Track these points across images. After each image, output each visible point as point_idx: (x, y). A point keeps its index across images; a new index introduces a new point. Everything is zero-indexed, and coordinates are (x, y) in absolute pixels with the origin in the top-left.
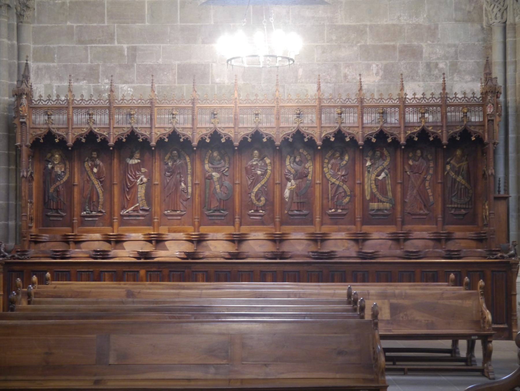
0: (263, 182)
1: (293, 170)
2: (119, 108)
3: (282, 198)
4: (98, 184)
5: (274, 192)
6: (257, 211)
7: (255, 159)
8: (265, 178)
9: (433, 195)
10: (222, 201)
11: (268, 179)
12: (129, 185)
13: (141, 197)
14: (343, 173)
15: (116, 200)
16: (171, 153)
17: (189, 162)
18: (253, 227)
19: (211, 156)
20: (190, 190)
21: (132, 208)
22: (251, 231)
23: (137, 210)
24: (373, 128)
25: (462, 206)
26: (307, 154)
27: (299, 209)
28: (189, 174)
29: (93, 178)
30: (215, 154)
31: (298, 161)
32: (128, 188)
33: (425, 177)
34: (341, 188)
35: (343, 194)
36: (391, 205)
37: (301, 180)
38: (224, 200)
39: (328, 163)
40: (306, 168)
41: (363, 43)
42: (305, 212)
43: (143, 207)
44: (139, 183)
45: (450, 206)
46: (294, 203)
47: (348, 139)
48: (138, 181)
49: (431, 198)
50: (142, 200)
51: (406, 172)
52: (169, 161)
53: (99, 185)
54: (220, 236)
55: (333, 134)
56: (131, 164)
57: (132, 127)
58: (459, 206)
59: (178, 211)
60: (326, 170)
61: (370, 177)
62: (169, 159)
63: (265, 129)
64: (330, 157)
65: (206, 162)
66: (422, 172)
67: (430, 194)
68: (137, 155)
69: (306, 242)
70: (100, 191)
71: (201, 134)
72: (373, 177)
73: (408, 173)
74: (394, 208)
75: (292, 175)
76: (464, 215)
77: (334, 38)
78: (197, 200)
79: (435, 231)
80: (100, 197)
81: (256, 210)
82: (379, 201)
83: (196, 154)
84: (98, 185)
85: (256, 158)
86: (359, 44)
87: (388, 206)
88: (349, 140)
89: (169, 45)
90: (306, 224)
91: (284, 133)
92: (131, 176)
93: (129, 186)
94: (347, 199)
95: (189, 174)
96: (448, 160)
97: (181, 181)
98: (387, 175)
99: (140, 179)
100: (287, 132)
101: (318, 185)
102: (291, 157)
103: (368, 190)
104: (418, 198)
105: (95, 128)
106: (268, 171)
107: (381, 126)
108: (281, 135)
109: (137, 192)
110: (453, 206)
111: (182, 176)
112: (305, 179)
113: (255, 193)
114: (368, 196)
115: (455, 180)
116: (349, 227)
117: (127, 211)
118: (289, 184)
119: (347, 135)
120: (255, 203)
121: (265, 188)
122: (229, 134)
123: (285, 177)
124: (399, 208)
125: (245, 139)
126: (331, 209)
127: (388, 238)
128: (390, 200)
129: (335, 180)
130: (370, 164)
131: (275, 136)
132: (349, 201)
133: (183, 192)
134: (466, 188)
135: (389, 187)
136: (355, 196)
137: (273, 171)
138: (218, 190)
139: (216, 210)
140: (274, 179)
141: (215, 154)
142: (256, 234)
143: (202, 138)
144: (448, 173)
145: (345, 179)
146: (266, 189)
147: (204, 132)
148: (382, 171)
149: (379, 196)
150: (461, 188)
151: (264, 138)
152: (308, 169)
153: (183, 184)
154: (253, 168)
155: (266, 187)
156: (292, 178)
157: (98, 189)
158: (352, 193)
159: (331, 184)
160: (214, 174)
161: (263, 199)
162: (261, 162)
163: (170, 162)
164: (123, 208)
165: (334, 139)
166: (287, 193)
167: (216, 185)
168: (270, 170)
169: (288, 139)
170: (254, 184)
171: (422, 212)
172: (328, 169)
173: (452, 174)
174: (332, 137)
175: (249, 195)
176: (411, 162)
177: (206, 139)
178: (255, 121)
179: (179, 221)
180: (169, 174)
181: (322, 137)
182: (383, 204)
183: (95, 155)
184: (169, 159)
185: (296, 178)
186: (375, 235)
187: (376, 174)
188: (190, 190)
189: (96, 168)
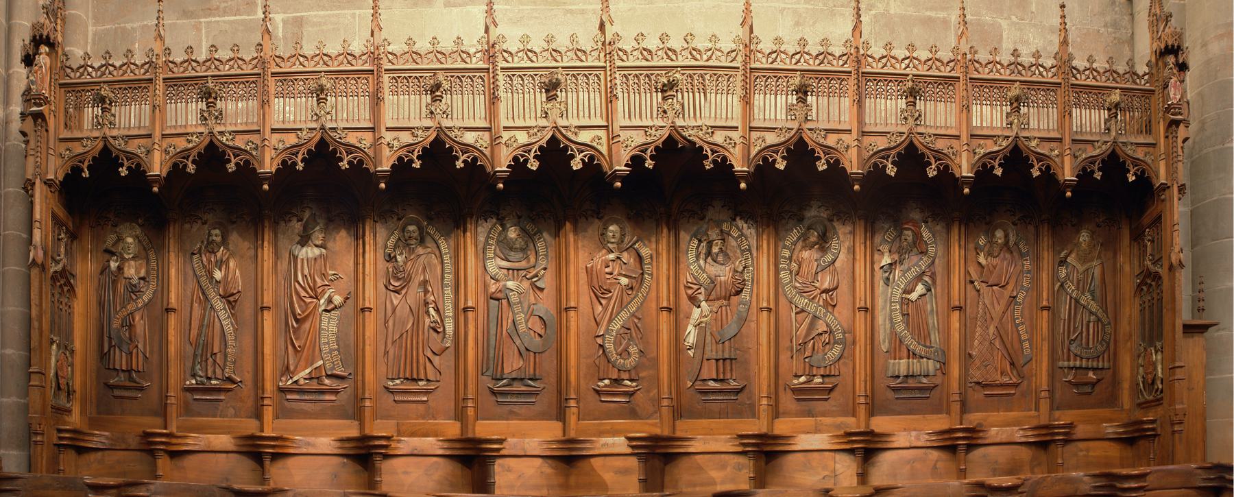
4: (224, 309)
5: (658, 331)
6: (617, 381)
8: (640, 295)
13: (328, 343)
15: (268, 349)
17: (446, 254)
20: (450, 327)
21: (308, 371)
27: (721, 377)
28: (447, 286)
29: (212, 294)
31: (717, 255)
32: (297, 321)
37: (725, 302)
42: (733, 384)
43: (333, 368)
44: (323, 308)
46: (708, 360)
48: (322, 301)
50: (331, 351)
51: (972, 282)
53: (227, 312)
56: (302, 260)
59: (422, 380)
66: (1007, 283)
72: (898, 293)
75: (702, 289)
80: (230, 343)
82: (911, 354)
93: (299, 314)
94: (836, 351)
95: (447, 286)
99: (326, 296)
102: (700, 241)
104: (997, 343)
110: (1072, 364)
113: (614, 334)
114: (884, 342)
115: (1077, 301)
117: (295, 379)
120: (615, 361)
121: (636, 321)
124: (955, 370)
134: (1099, 320)
135: (932, 321)
139: (514, 379)
141: (512, 233)
144: (1062, 285)
145: (832, 299)
149: (909, 340)
150: (1089, 322)
153: (432, 311)
155: (639, 319)
156: (701, 297)
159: (797, 313)
160: (510, 284)
163: (401, 254)
164: (286, 371)
166: (691, 335)
167: (518, 313)
168: (649, 274)
171: (1005, 380)
176: (982, 260)
179: (421, 407)
184: (395, 247)
188: (450, 327)
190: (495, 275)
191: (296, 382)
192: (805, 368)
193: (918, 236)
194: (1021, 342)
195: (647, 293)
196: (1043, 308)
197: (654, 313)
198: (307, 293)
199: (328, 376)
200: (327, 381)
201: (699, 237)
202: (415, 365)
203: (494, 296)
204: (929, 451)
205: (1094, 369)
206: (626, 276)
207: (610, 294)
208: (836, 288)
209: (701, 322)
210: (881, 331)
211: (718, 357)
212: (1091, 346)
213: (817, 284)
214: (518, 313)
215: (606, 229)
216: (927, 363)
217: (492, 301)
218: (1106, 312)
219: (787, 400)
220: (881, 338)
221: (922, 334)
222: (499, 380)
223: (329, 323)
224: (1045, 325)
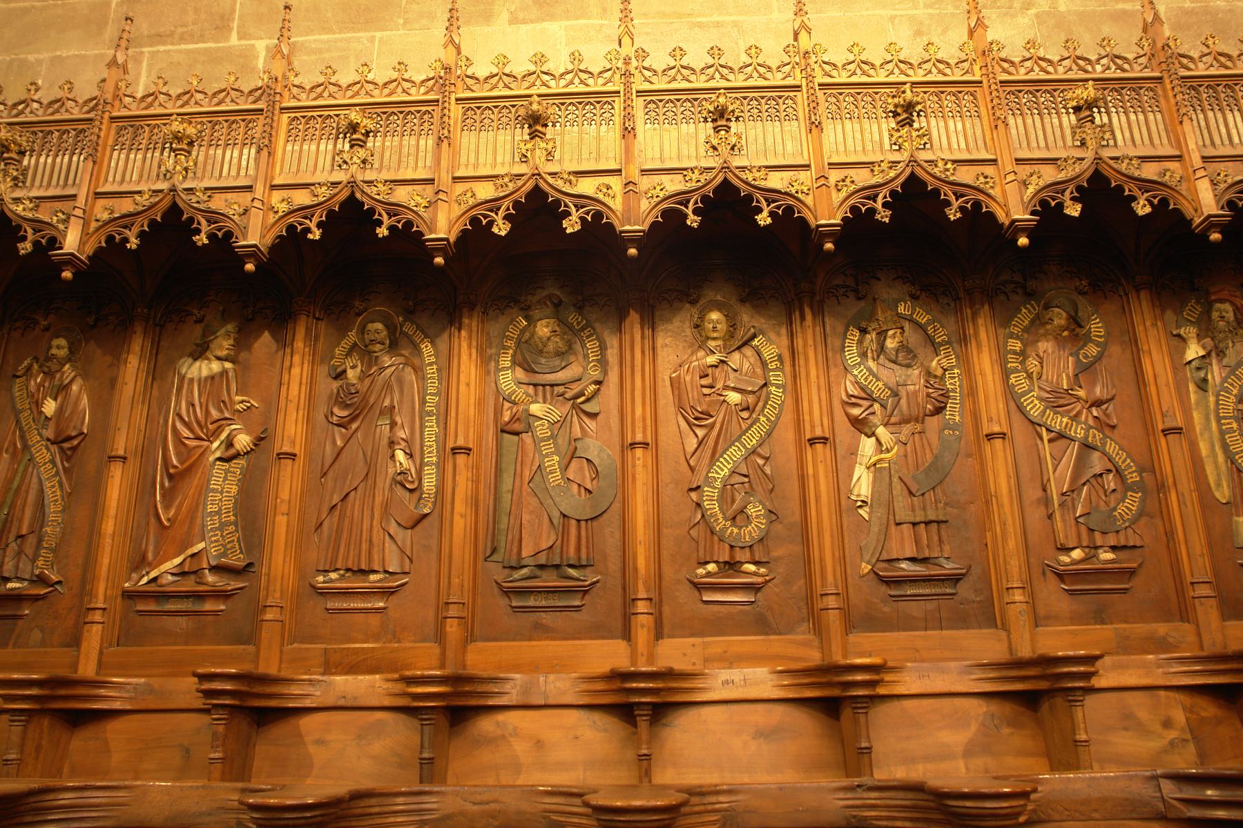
0: (751, 439)
1: (881, 384)
2: (133, 122)
3: (844, 504)
4: (53, 461)
6: (731, 566)
7: (712, 344)
8: (762, 418)
10: (573, 522)
11: (773, 426)
12: (175, 462)
13: (219, 513)
14: (1098, 392)
15: (109, 526)
16: (363, 330)
17: (431, 364)
18: (718, 644)
19: (527, 335)
21: (177, 561)
22: (707, 660)
23: (195, 572)
26: (929, 323)
28: (430, 414)
30: (543, 329)
32: (171, 477)
34: (1096, 455)
37: (919, 427)
38: (579, 521)
39: (1023, 354)
40: (936, 377)
42: (949, 567)
43: (224, 555)
44: (218, 454)
48: (216, 444)
50: (222, 526)
52: (349, 363)
53: (55, 465)
54: (559, 686)
55: (1071, 187)
56: (192, 380)
57: (173, 189)
60: (1018, 381)
61: (1212, 406)
62: (349, 354)
64: (1026, 330)
65: (506, 361)
68: (223, 345)
69: (978, 708)
70: (53, 494)
71: (471, 202)
75: (876, 406)
78: (460, 524)
81: (726, 563)
83: (460, 330)
84: (49, 466)
85: (714, 339)
86: (1032, 11)
89: (401, 32)
90: (961, 620)
91: (852, 188)
92: (187, 425)
93: (175, 467)
94: (1130, 504)
95: (430, 414)
97: (392, 443)
99: (223, 436)
100: (861, 185)
102: (864, 331)
105: (17, 200)
106: (773, 389)
108: (837, 197)
109: (204, 489)
111: (398, 419)
112: (933, 422)
113: (718, 484)
114: (1219, 485)
116: (1162, 629)
117: (153, 574)
118: (867, 445)
119: (1137, 192)
120: (725, 528)
121: (761, 462)
122: (600, 196)
123: (847, 415)
125: (671, 218)
129: (1065, 420)
131: (809, 200)
132: (1142, 513)
133: (399, 489)
136: (1161, 487)
138: (555, 478)
141: (543, 329)
142: (736, 674)
143: (474, 221)
145: (1107, 416)
146: (768, 470)
147: (485, 191)
151: (760, 210)
152: (942, 378)
153: (400, 455)
154: (704, 382)
155: (767, 459)
157: (47, 484)
158: (1144, 474)
159: (1050, 441)
160: (535, 409)
162: (736, 355)
163: (353, 367)
164: (140, 562)
165: (1079, 207)
166: (863, 484)
167: (547, 455)
168: (778, 386)
169: (872, 211)
172: (1030, 376)
175: (694, 495)
177: (491, 223)
178: (715, 142)
179: (374, 620)
180: (345, 413)
183: (58, 347)
185: (893, 420)
187: (1235, 392)
189: (55, 399)
190: (510, 395)
191: (155, 579)
192: (1079, 536)
195: (778, 417)
197: (792, 449)
198: (191, 430)
199: (215, 569)
200: (210, 578)
201: (863, 324)
202: (364, 546)
203: (506, 428)
206: (735, 389)
207: (711, 420)
208: (1112, 399)
210: (1209, 470)
211: (918, 520)
213: (1081, 393)
214: (547, 455)
215: (702, 318)
217: (506, 436)
219: (1053, 595)
220: (1212, 480)
222: (512, 568)
223: (225, 479)
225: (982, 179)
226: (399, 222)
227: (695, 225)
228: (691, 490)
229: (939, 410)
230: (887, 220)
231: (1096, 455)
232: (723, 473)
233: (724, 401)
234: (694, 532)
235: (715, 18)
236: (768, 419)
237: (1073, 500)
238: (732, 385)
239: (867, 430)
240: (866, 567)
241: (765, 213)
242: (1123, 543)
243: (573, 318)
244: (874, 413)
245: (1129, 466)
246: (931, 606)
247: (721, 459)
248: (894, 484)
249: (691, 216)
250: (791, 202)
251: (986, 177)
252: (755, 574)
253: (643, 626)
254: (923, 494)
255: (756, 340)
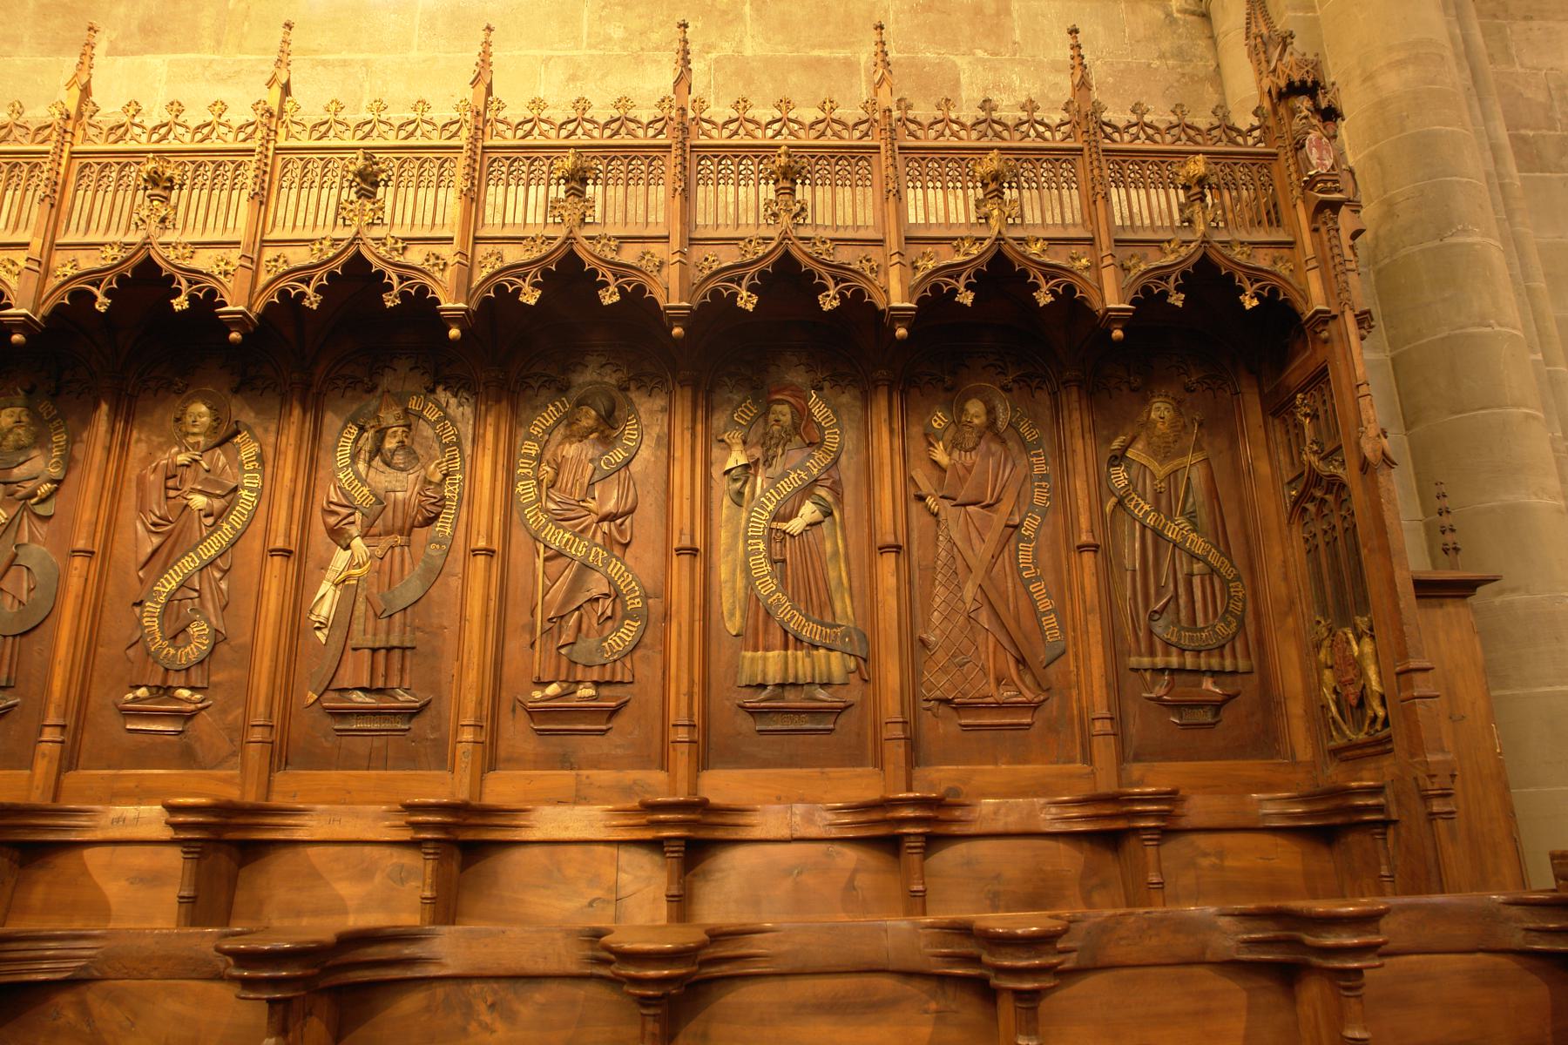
0: (210, 549)
1: (366, 490)
5: (259, 594)
8: (226, 526)
9: (1059, 612)
24: (742, 244)
25: (1203, 663)
27: (380, 684)
33: (1017, 520)
35: (606, 606)
36: (852, 665)
37: (400, 539)
41: (727, 48)
42: (404, 699)
45: (1146, 661)
46: (355, 649)
47: (609, 297)
49: (1050, 622)
51: (921, 498)
58: (1189, 661)
63: (187, 252)
66: (998, 500)
67: (1044, 604)
72: (761, 520)
73: (930, 500)
74: (865, 664)
75: (358, 515)
76: (1217, 706)
77: (617, 32)
79: (1084, 790)
81: (159, 688)
82: (791, 640)
85: (194, 434)
86: (713, 55)
87: (836, 664)
88: (616, 298)
94: (627, 633)
96: (1116, 444)
98: (828, 513)
100: (293, 265)
101: (481, 560)
102: (362, 429)
103: (734, 589)
104: (984, 618)
107: (785, 237)
110: (1159, 661)
113: (162, 599)
114: (732, 614)
115: (1158, 534)
118: (341, 558)
119: (610, 278)
121: (218, 575)
123: (325, 523)
124: (891, 673)
126: (542, 684)
127: (835, 833)
128: (847, 634)
130: (743, 461)
134: (1213, 571)
135: (837, 573)
137: (265, 495)
140: (267, 531)
142: (130, 811)
144: (1120, 503)
145: (621, 533)
146: (223, 585)
148: (806, 491)
149: (785, 611)
150: (1190, 575)
151: (178, 293)
155: (225, 572)
156: (354, 530)
159: (546, 560)
161: (199, 631)
166: (326, 601)
168: (251, 490)
170: (159, 561)
171: (1007, 694)
173: (1142, 507)
174: (527, 288)
175: (137, 610)
176: (940, 455)
181: (475, 284)
182: (808, 655)
186: (769, 822)
187: (771, 507)
192: (558, 668)
193: (802, 416)
194: (1036, 615)
196: (1081, 548)
204: (837, 847)
205: (1213, 673)
206: (201, 492)
208: (631, 511)
209: (349, 577)
211: (377, 645)
212: (1200, 624)
213: (592, 505)
216: (828, 659)
218: (1227, 553)
220: (726, 607)
221: (814, 599)
224: (1089, 582)
225: (432, 260)
226: (111, 283)
227: (102, 309)
228: (135, 604)
229: (429, 521)
230: (315, 307)
231: (597, 575)
232: (169, 587)
233: (187, 505)
234: (131, 652)
235: (345, 55)
236: (233, 528)
237: (560, 627)
238: (199, 487)
239: (342, 542)
240: (311, 697)
241: (183, 297)
242: (607, 678)
243: (44, 407)
244: (353, 523)
245: (633, 591)
246: (377, 742)
247: (171, 571)
248: (358, 604)
249: (101, 298)
250: (214, 284)
251: (437, 258)
252: (187, 700)
253: (44, 755)
254: (390, 616)
255: (239, 436)
